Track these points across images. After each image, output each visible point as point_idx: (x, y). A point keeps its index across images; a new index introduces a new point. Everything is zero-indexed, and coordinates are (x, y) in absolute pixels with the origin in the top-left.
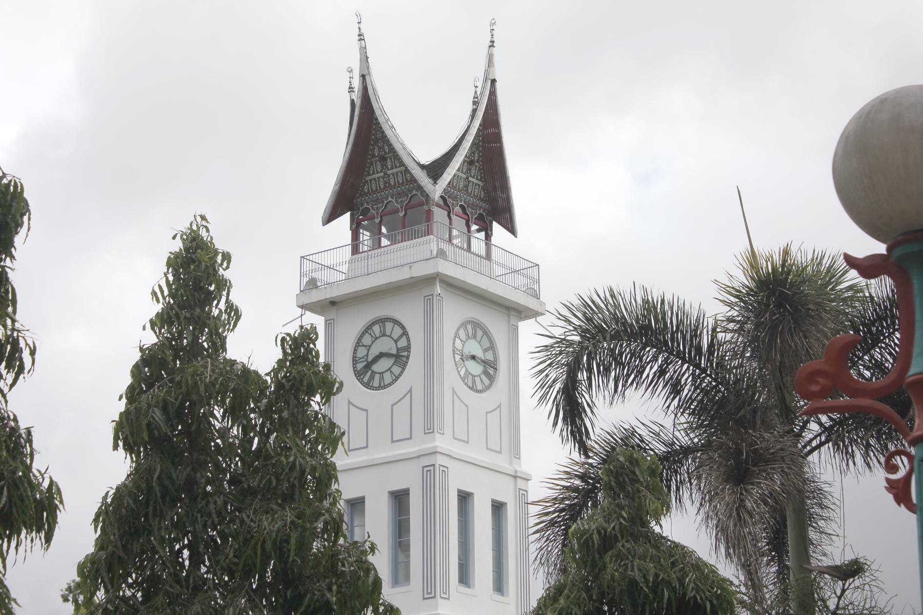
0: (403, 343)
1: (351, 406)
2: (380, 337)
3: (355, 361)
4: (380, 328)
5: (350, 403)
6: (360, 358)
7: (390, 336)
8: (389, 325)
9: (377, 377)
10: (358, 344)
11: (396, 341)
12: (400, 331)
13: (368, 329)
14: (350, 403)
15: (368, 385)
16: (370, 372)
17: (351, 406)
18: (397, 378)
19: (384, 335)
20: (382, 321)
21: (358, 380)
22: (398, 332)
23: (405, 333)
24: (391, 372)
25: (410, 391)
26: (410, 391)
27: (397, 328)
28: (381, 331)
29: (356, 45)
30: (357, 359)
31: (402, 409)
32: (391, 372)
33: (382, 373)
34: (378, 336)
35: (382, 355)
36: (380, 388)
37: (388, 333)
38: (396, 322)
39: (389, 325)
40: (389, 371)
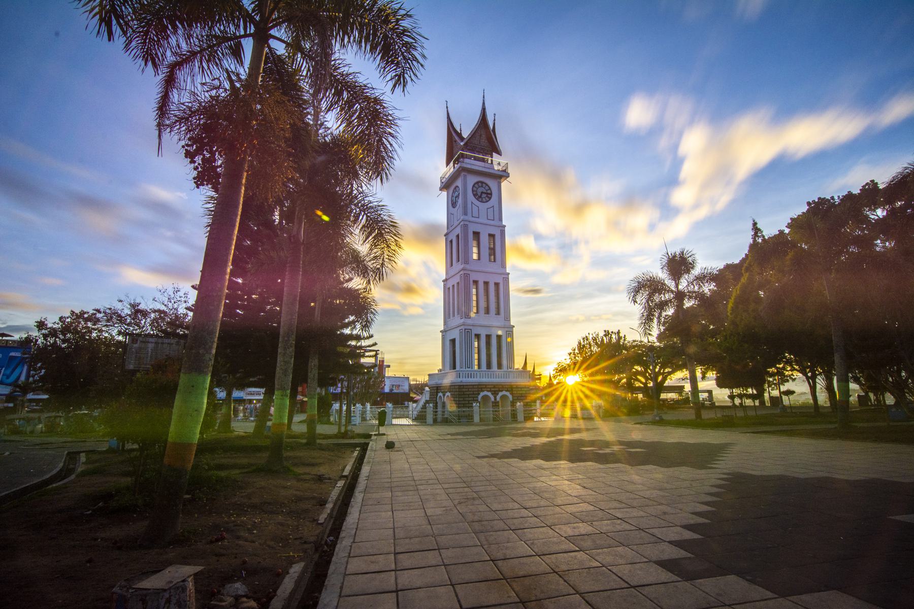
3: (473, 191)
5: (472, 203)
8: (484, 185)
10: (474, 186)
13: (477, 183)
14: (472, 203)
17: (473, 205)
18: (487, 201)
19: (482, 186)
20: (482, 183)
22: (487, 188)
23: (490, 189)
25: (493, 206)
26: (493, 206)
27: (487, 187)
29: (482, 99)
35: (482, 193)
37: (484, 186)
38: (487, 185)
39: (484, 185)
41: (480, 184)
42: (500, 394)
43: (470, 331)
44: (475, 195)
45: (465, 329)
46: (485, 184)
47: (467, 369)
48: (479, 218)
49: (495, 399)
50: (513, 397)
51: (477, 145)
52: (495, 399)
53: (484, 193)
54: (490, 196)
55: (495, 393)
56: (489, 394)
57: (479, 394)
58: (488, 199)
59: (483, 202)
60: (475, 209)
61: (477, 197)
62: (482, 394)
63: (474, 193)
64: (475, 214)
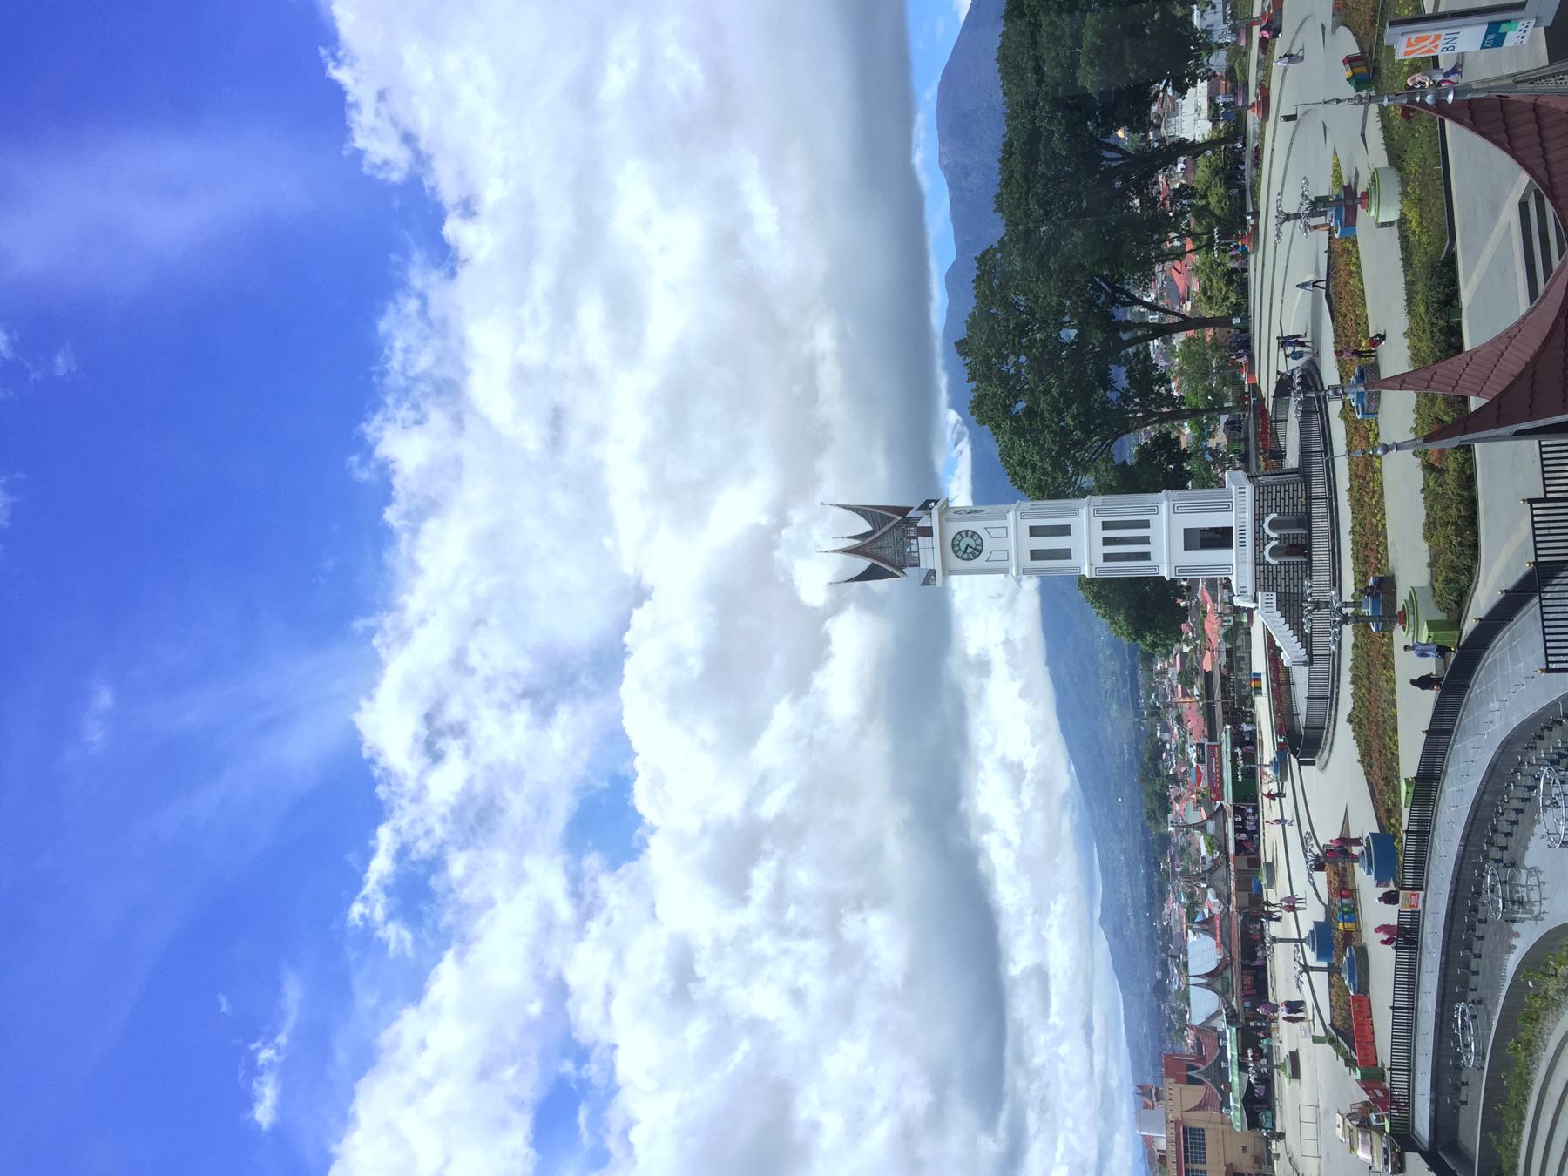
3: (969, 559)
8: (956, 542)
9: (978, 547)
10: (962, 558)
12: (959, 536)
13: (955, 552)
19: (959, 545)
20: (953, 545)
22: (959, 537)
23: (959, 533)
31: (994, 532)
39: (956, 542)
41: (956, 549)
42: (1268, 531)
46: (953, 541)
49: (1276, 539)
50: (1272, 512)
52: (1276, 539)
53: (971, 547)
54: (970, 534)
55: (1270, 539)
56: (1268, 548)
57: (1268, 564)
58: (976, 536)
62: (1268, 559)
64: (1003, 555)
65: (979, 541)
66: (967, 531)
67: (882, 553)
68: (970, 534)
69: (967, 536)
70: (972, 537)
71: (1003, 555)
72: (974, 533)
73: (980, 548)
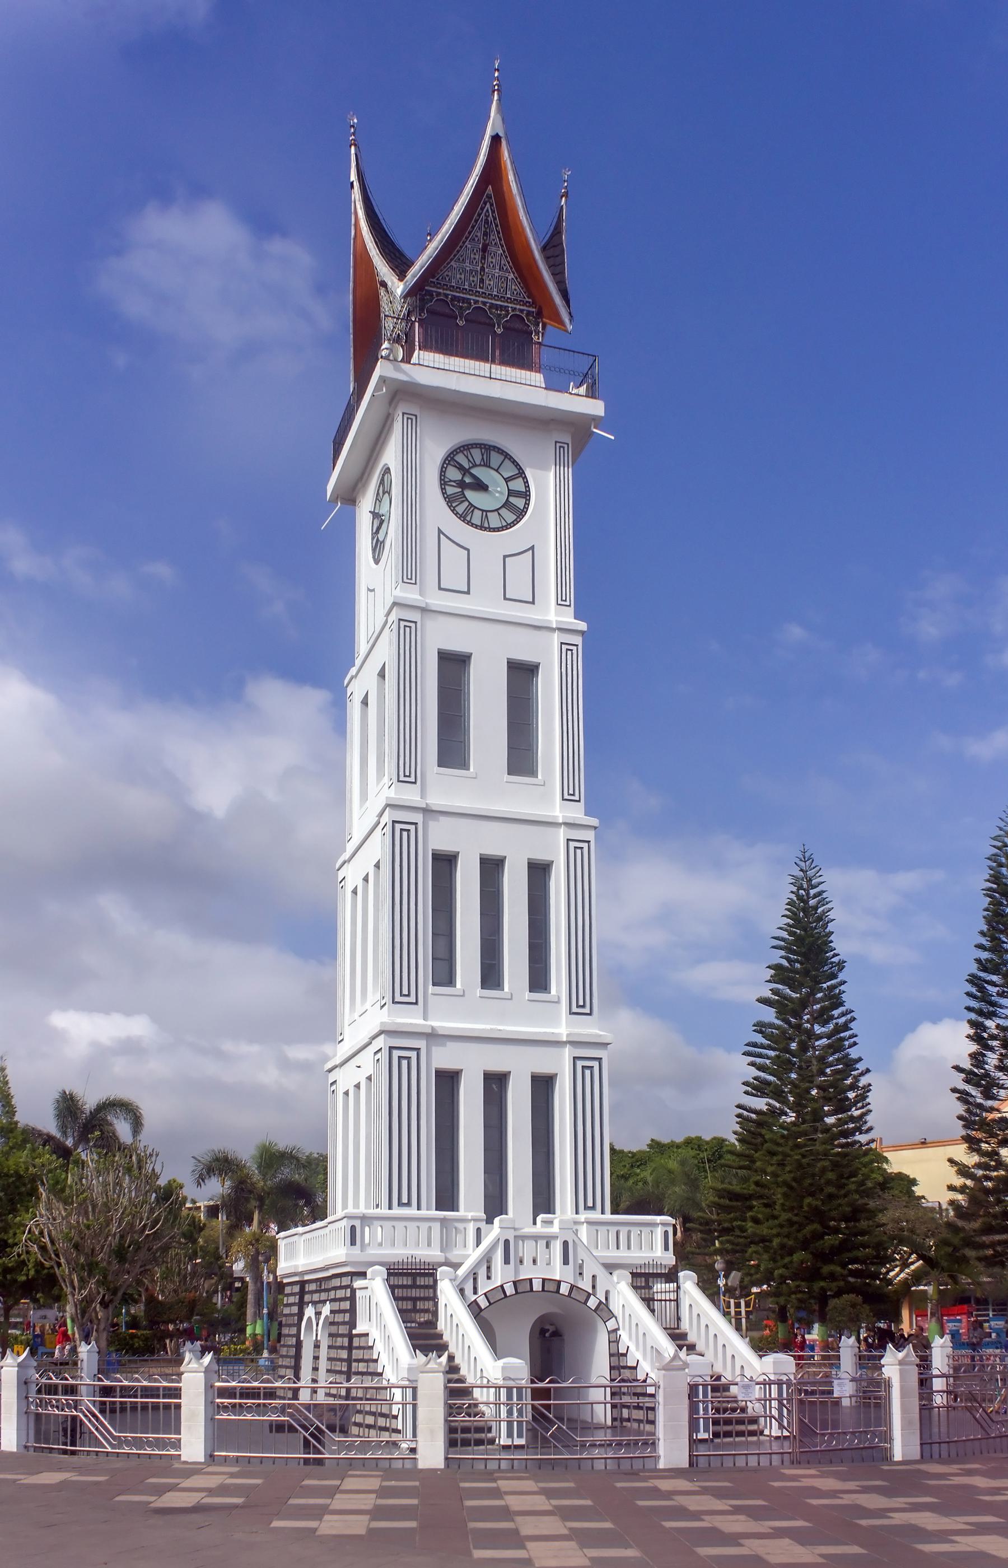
0: (518, 485)
1: (441, 536)
2: (480, 465)
3: (444, 482)
4: (483, 455)
5: (440, 532)
6: (451, 481)
7: (497, 471)
8: (496, 459)
9: (477, 514)
11: (507, 480)
13: (465, 448)
14: (440, 532)
15: (462, 517)
16: (466, 504)
17: (441, 536)
20: (487, 449)
21: (450, 507)
22: (509, 471)
23: (521, 474)
24: (499, 514)
25: (532, 548)
26: (532, 548)
28: (483, 458)
30: (446, 480)
32: (499, 514)
33: (487, 511)
34: (478, 463)
36: (482, 527)
37: (494, 463)
38: (507, 456)
39: (496, 459)
40: (496, 513)
41: (477, 454)
43: (413, 1055)
44: (450, 501)
45: (391, 1048)
47: (397, 1211)
48: (468, 592)
51: (470, 292)
54: (519, 503)
58: (510, 517)
59: (491, 529)
60: (453, 558)
61: (460, 509)
63: (450, 490)
64: (454, 578)
65: (494, 521)
66: (526, 495)
67: (470, 249)
68: (519, 503)
69: (511, 493)
70: (507, 505)
71: (454, 578)
72: (521, 513)
73: (477, 520)
